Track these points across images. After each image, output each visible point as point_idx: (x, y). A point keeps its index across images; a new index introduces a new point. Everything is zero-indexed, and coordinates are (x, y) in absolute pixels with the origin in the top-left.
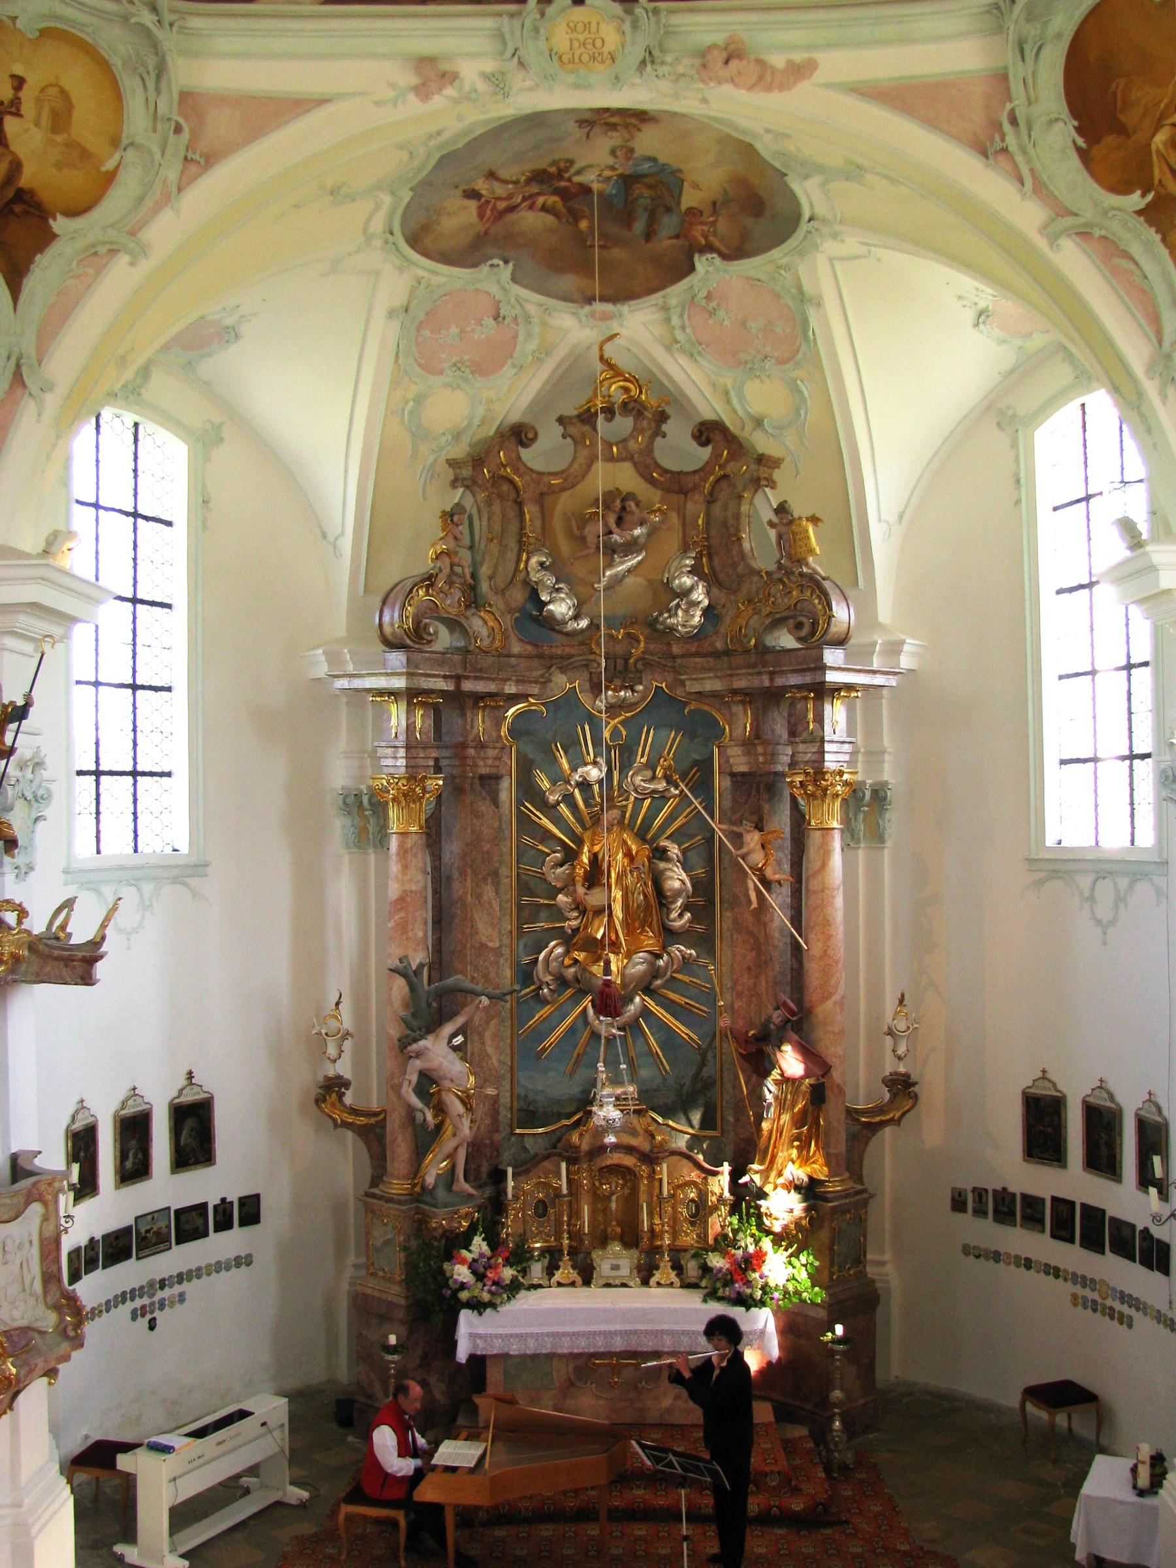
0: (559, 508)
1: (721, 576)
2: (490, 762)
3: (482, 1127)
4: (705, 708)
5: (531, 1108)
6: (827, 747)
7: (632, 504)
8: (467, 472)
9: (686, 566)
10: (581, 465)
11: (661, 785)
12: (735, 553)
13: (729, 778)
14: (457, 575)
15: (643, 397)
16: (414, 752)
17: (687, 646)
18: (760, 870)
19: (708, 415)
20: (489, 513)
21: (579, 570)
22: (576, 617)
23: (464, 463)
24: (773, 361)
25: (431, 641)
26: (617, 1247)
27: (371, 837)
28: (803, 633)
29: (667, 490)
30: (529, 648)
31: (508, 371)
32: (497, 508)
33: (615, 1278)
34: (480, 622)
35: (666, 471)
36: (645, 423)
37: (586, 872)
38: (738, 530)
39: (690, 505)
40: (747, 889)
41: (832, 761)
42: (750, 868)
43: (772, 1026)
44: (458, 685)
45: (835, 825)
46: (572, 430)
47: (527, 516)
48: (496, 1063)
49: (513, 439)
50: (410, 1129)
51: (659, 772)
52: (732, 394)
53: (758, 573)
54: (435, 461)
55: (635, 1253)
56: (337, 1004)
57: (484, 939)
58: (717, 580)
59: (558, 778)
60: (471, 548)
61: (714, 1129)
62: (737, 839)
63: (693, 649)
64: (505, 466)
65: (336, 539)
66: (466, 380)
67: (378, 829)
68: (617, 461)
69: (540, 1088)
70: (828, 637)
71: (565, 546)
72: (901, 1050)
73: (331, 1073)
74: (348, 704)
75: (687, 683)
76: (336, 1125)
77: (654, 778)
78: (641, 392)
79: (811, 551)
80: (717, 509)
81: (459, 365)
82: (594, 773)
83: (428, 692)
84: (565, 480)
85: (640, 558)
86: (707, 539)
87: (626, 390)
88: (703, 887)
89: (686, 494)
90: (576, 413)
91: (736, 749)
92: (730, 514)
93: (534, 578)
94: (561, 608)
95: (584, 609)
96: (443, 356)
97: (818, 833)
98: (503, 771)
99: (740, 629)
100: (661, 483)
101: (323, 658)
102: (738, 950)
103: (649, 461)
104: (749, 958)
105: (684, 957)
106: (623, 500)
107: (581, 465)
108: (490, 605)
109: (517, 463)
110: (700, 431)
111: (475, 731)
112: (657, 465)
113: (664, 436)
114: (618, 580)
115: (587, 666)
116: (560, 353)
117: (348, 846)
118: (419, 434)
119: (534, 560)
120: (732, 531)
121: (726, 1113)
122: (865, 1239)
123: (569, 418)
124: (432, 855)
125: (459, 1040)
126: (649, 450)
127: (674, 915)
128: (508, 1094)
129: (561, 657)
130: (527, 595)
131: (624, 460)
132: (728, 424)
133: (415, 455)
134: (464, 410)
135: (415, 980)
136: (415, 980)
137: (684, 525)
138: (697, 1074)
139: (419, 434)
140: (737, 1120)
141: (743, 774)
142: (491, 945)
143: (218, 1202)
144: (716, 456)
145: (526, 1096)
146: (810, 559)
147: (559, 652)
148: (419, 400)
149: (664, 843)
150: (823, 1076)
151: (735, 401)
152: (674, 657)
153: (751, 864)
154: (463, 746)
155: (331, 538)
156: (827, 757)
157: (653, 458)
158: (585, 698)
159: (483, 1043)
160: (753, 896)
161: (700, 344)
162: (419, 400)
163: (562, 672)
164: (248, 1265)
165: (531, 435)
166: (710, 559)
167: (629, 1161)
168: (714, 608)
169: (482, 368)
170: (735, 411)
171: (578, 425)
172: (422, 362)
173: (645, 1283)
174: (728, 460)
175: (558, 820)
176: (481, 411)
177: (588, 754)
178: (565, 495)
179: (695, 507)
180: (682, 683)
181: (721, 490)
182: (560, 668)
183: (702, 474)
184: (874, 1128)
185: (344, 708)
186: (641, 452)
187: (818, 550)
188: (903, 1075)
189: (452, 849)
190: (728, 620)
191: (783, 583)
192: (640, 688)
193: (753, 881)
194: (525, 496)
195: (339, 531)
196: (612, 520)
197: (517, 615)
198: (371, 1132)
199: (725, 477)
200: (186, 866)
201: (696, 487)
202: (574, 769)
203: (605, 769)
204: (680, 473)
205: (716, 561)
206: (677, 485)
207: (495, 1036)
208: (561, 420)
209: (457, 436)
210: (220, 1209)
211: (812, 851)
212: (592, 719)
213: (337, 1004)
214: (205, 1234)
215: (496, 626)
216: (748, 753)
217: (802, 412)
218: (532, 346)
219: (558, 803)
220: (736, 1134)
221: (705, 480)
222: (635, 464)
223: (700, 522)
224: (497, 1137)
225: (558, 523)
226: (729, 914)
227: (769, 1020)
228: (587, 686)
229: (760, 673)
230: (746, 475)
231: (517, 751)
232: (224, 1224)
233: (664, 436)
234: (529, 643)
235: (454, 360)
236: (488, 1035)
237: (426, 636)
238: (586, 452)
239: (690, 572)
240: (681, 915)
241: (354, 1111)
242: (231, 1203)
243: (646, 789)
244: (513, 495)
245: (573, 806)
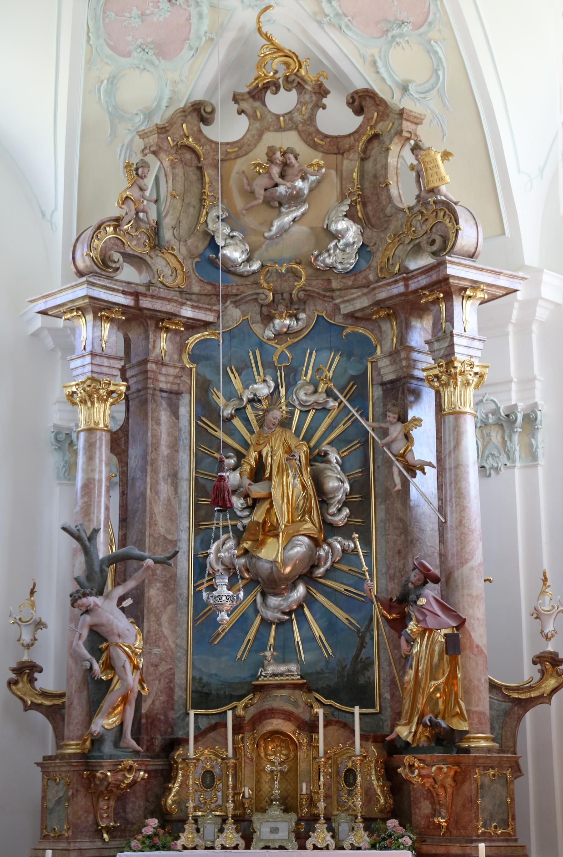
0: (234, 175)
1: (374, 220)
2: (171, 379)
3: (157, 702)
4: (361, 331)
5: (205, 690)
6: (456, 340)
7: (291, 156)
8: (153, 139)
9: (343, 211)
10: (253, 136)
11: (321, 398)
12: (384, 197)
13: (380, 388)
14: (142, 220)
15: (303, 72)
16: (98, 360)
17: (344, 281)
18: (403, 455)
19: (360, 85)
20: (173, 173)
21: (250, 221)
22: (248, 260)
23: (151, 132)
24: (410, 26)
25: (118, 269)
26: (275, 811)
28: (435, 248)
29: (326, 153)
30: (209, 288)
31: (186, 54)
32: (179, 170)
33: (274, 841)
34: (164, 263)
35: (326, 136)
36: (307, 97)
37: (252, 469)
38: (386, 177)
39: (346, 162)
40: (392, 474)
41: (461, 352)
42: (395, 456)
43: (410, 586)
44: (137, 301)
45: (467, 409)
46: (245, 105)
47: (207, 179)
48: (173, 646)
49: (195, 114)
50: (85, 693)
51: (322, 387)
52: (380, 64)
53: (402, 210)
54: (132, 140)
55: (293, 817)
56: (32, 592)
57: (162, 531)
58: (370, 223)
59: (231, 395)
60: (156, 201)
61: (373, 707)
62: (384, 433)
63: (350, 283)
64: (188, 137)
66: (152, 64)
68: (284, 131)
69: (213, 671)
70: (457, 248)
71: (239, 203)
72: (549, 629)
73: (25, 658)
75: (342, 306)
76: (27, 708)
77: (315, 392)
78: (300, 67)
79: (441, 179)
80: (369, 165)
81: (144, 47)
82: (263, 390)
83: (110, 306)
84: (240, 148)
85: (302, 210)
86: (361, 189)
87: (287, 65)
88: (360, 486)
89: (342, 154)
90: (247, 90)
91: (385, 360)
92: (379, 166)
93: (211, 227)
94: (235, 253)
95: (256, 255)
96: (129, 38)
97: (452, 417)
98: (182, 388)
99: (388, 260)
100: (322, 146)
102: (390, 537)
103: (312, 129)
104: (399, 542)
105: (344, 551)
106: (284, 154)
107: (253, 136)
108: (173, 249)
109: (199, 136)
110: (352, 97)
111: (157, 351)
112: (318, 132)
113: (324, 107)
114: (283, 231)
115: (256, 300)
116: (230, 36)
117: (58, 478)
118: (117, 115)
119: (213, 214)
120: (382, 180)
121: (383, 691)
122: (513, 800)
123: (242, 95)
124: (120, 461)
125: (128, 603)
126: (312, 119)
127: (333, 510)
128: (184, 676)
129: (236, 295)
130: (207, 243)
131: (290, 129)
132: (377, 90)
133: (114, 134)
134: (154, 89)
135: (87, 543)
136: (87, 543)
137: (341, 180)
138: (357, 656)
139: (117, 115)
140: (393, 695)
141: (392, 382)
142: (169, 537)
144: (368, 120)
145: (201, 679)
146: (443, 189)
147: (235, 291)
148: (113, 80)
149: (325, 447)
150: (457, 628)
151: (382, 70)
152: (333, 291)
153: (395, 453)
154: (145, 362)
155: (48, 216)
156: (457, 349)
157: (315, 126)
158: (257, 328)
159: (160, 625)
160: (397, 480)
161: (346, 16)
162: (113, 80)
163: (236, 307)
165: (209, 109)
166: (364, 205)
167: (288, 727)
168: (368, 246)
169: (162, 50)
170: (383, 80)
171: (251, 100)
172: (111, 43)
173: (302, 847)
174: (376, 123)
175: (232, 432)
176: (167, 94)
177: (259, 375)
178: (239, 161)
179: (351, 164)
180: (337, 308)
181: (373, 148)
182: (234, 303)
183: (357, 136)
184: (525, 704)
186: (304, 123)
187: (448, 179)
188: (551, 653)
189: (134, 452)
190: (379, 254)
191: (422, 213)
192: (302, 316)
193: (398, 466)
194: (205, 162)
196: (276, 171)
197: (197, 260)
198: (55, 711)
199: (376, 136)
201: (351, 148)
202: (246, 387)
203: (272, 384)
204: (336, 137)
205: (369, 208)
206: (335, 146)
207: (172, 620)
208: (236, 99)
209: (149, 115)
211: (448, 436)
212: (261, 345)
213: (32, 592)
215: (178, 267)
216: (393, 363)
217: (440, 73)
218: (205, 26)
219: (232, 417)
220: (392, 709)
221: (358, 141)
222: (299, 133)
223: (355, 175)
224: (172, 715)
225: (233, 184)
226: (383, 507)
227: (408, 581)
228: (258, 318)
229: (396, 282)
230: (393, 131)
231: (197, 374)
233: (324, 107)
234: (209, 283)
235: (139, 41)
236: (165, 618)
237: (110, 264)
238: (257, 125)
239: (345, 216)
240: (339, 510)
241: (44, 694)
243: (306, 402)
244: (195, 162)
245: (246, 421)
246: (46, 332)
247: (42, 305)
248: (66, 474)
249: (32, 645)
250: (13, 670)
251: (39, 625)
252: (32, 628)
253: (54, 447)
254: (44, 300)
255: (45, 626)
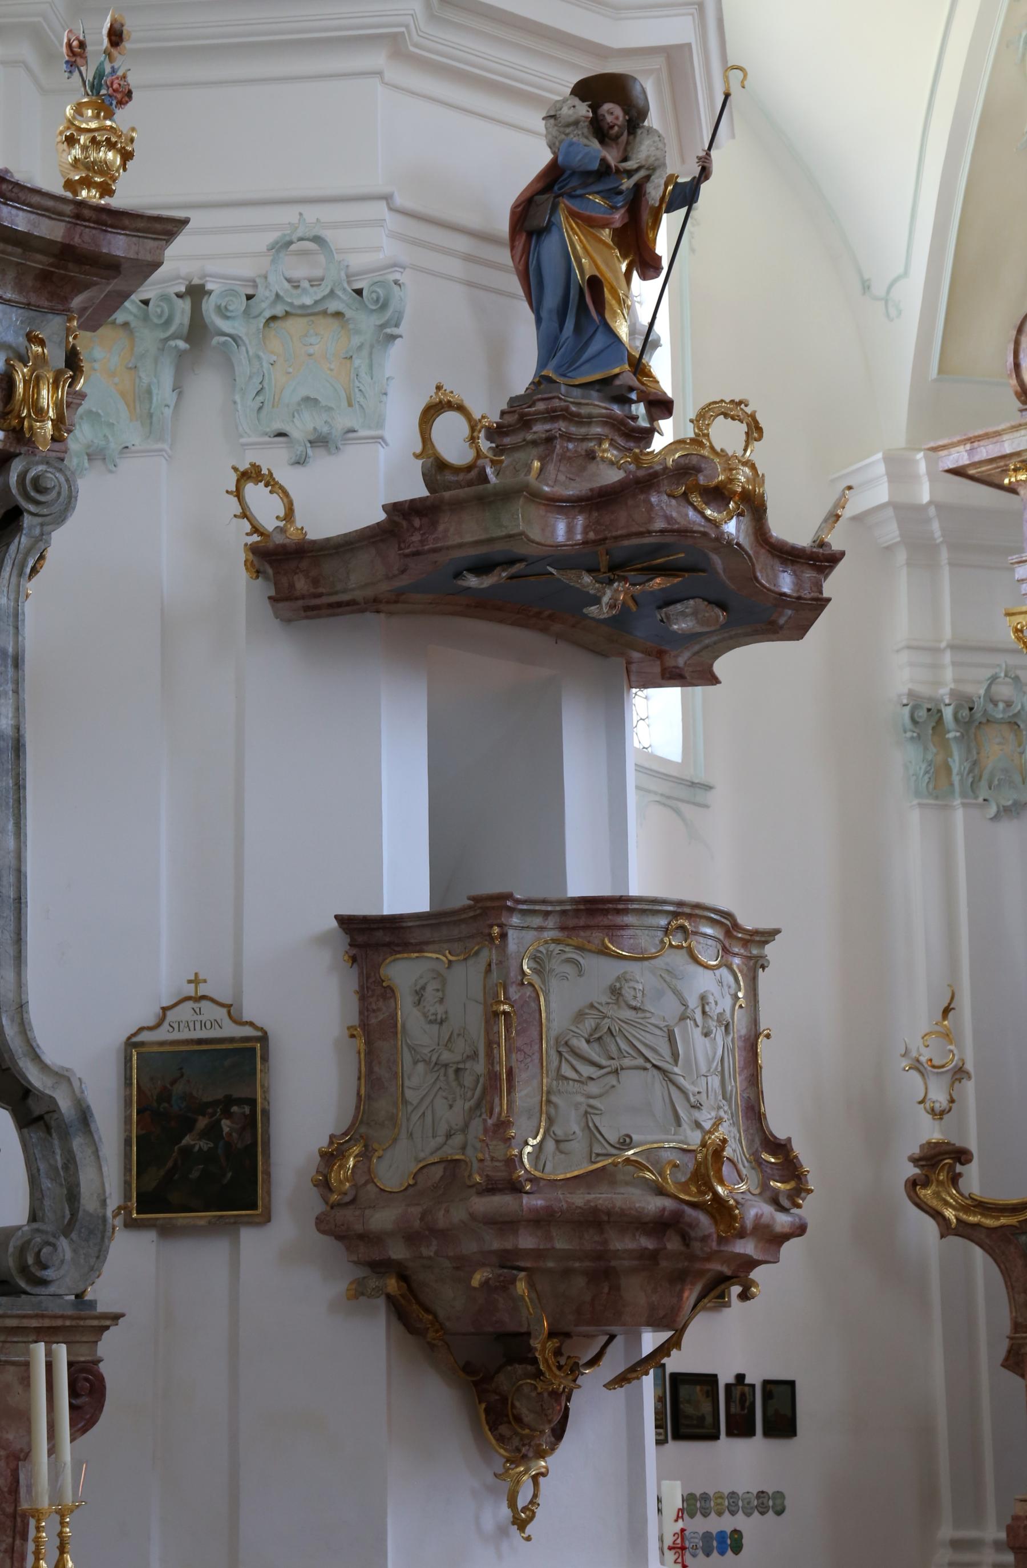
27: (956, 779)
65: (888, 292)
67: (967, 765)
73: (936, 1136)
74: (909, 564)
101: (881, 469)
117: (917, 794)
143: (731, 1380)
155: (879, 289)
164: (779, 1513)
185: (904, 573)
195: (901, 270)
200: (679, 781)
210: (737, 1392)
214: (715, 1437)
232: (741, 1428)
242: (753, 1386)
246: (890, 512)
247: (959, 457)
248: (931, 786)
249: (950, 1111)
250: (915, 1160)
251: (960, 1073)
252: (947, 1079)
253: (909, 734)
254: (968, 446)
255: (968, 1075)
